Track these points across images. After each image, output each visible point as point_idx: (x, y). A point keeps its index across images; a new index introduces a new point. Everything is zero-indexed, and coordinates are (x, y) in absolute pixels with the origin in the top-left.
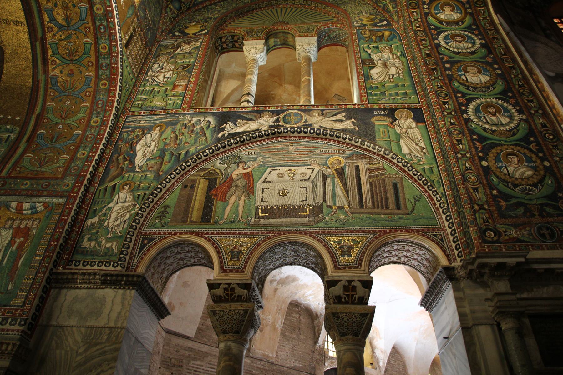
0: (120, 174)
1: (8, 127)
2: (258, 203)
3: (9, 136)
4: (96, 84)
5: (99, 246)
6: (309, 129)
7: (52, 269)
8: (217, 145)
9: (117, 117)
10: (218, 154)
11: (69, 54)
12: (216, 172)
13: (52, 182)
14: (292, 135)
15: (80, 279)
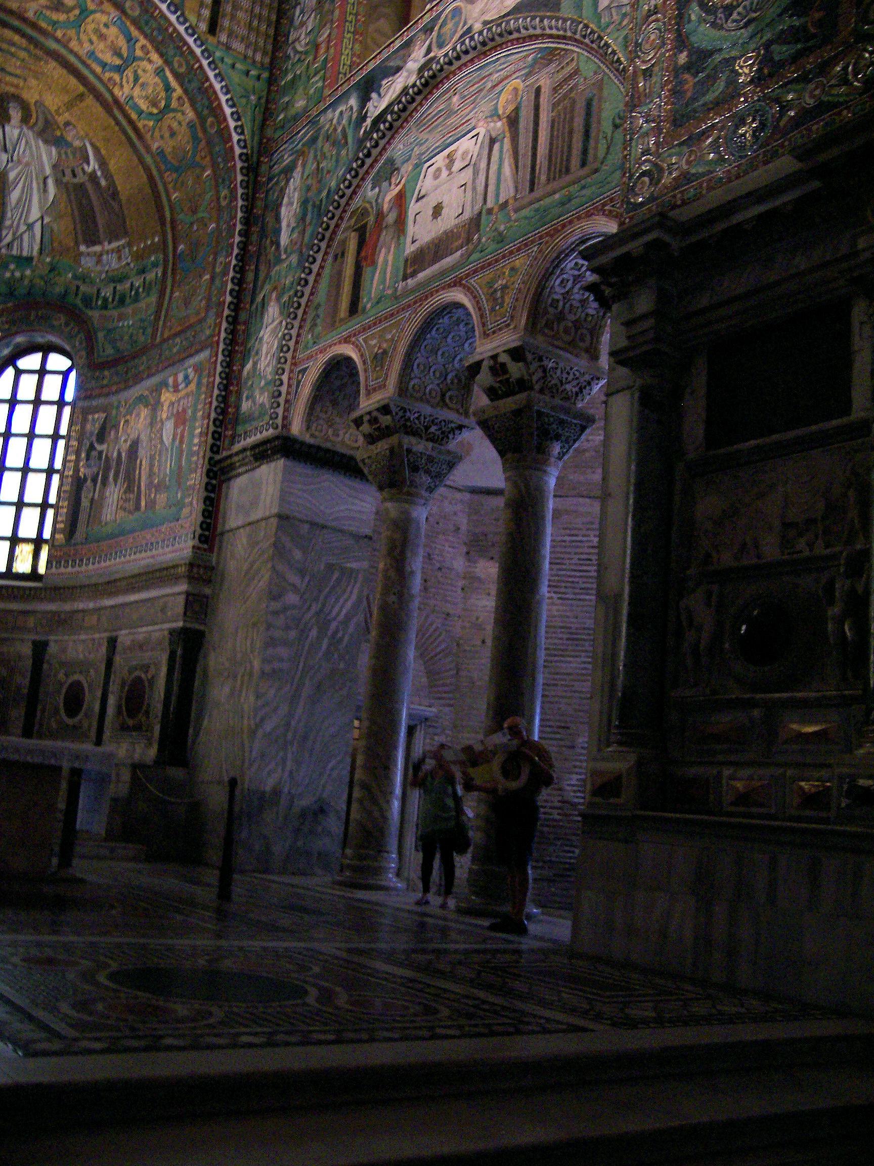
0: (268, 276)
1: (153, 259)
2: (410, 249)
3: (157, 274)
4: (205, 131)
5: (255, 404)
6: (467, 41)
7: (211, 459)
8: (358, 158)
9: (252, 169)
10: (367, 173)
11: (154, 104)
12: (365, 209)
13: (198, 328)
14: (453, 68)
15: (239, 461)
